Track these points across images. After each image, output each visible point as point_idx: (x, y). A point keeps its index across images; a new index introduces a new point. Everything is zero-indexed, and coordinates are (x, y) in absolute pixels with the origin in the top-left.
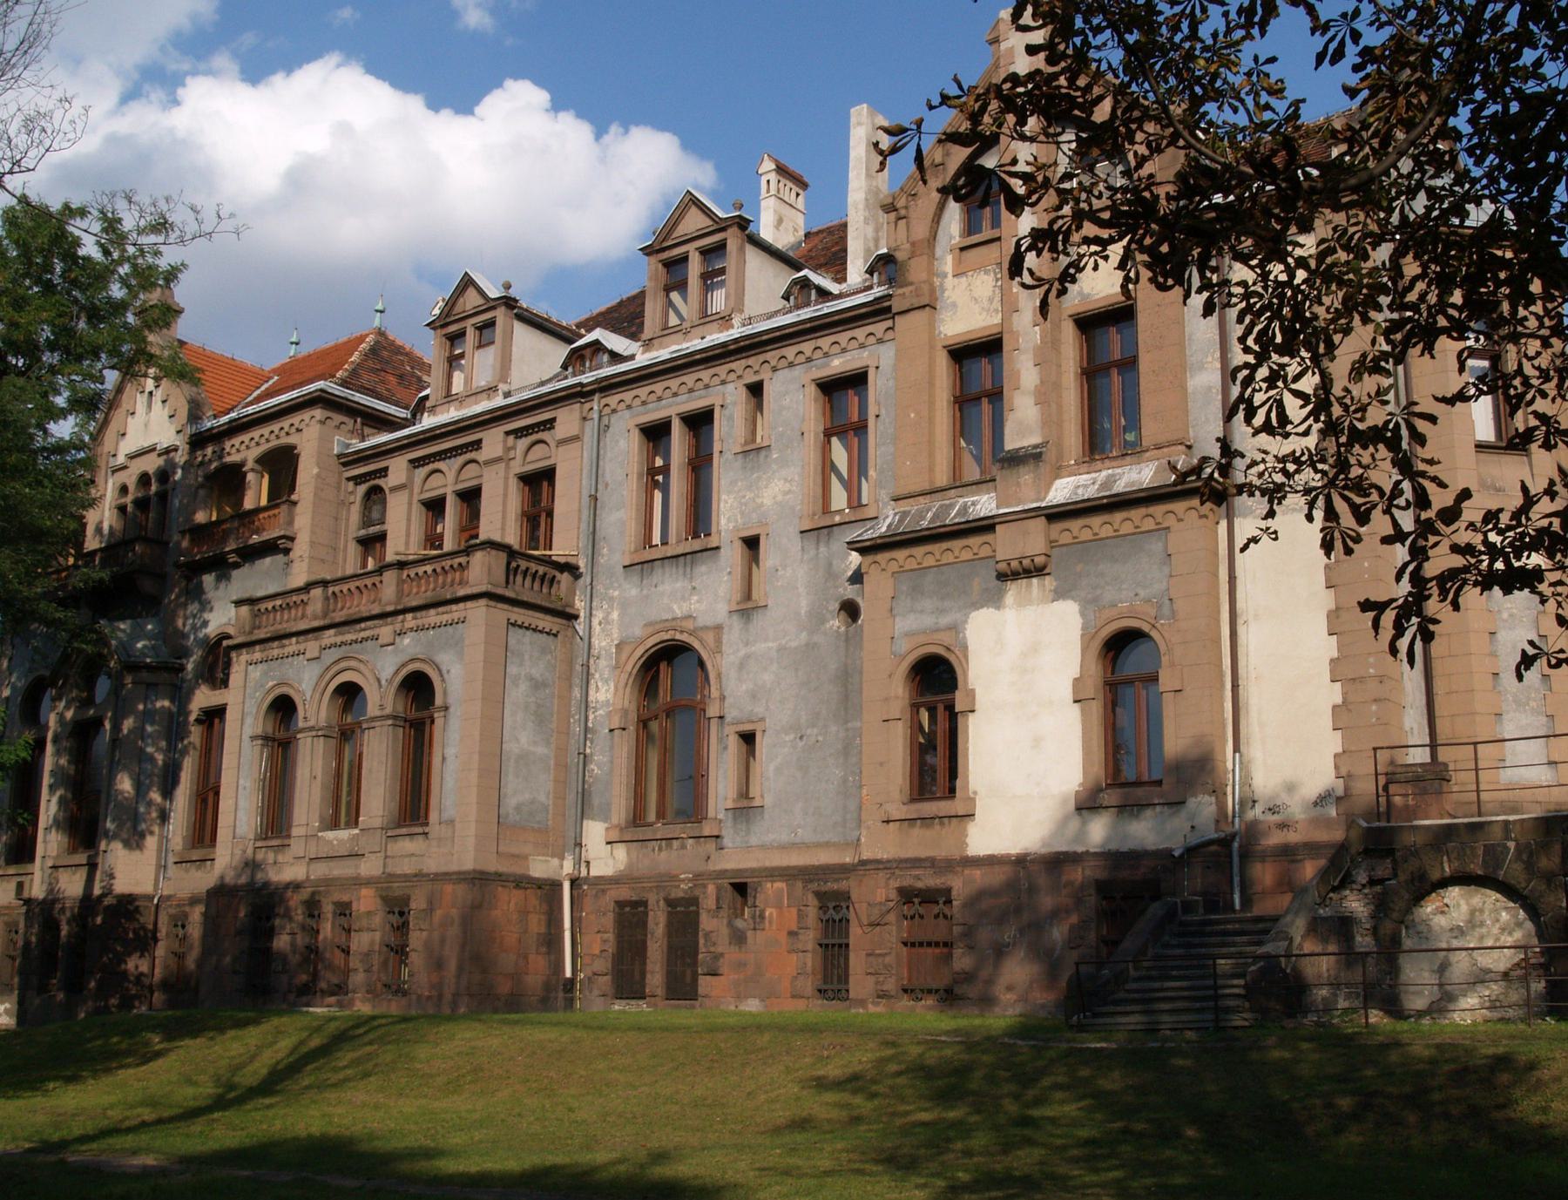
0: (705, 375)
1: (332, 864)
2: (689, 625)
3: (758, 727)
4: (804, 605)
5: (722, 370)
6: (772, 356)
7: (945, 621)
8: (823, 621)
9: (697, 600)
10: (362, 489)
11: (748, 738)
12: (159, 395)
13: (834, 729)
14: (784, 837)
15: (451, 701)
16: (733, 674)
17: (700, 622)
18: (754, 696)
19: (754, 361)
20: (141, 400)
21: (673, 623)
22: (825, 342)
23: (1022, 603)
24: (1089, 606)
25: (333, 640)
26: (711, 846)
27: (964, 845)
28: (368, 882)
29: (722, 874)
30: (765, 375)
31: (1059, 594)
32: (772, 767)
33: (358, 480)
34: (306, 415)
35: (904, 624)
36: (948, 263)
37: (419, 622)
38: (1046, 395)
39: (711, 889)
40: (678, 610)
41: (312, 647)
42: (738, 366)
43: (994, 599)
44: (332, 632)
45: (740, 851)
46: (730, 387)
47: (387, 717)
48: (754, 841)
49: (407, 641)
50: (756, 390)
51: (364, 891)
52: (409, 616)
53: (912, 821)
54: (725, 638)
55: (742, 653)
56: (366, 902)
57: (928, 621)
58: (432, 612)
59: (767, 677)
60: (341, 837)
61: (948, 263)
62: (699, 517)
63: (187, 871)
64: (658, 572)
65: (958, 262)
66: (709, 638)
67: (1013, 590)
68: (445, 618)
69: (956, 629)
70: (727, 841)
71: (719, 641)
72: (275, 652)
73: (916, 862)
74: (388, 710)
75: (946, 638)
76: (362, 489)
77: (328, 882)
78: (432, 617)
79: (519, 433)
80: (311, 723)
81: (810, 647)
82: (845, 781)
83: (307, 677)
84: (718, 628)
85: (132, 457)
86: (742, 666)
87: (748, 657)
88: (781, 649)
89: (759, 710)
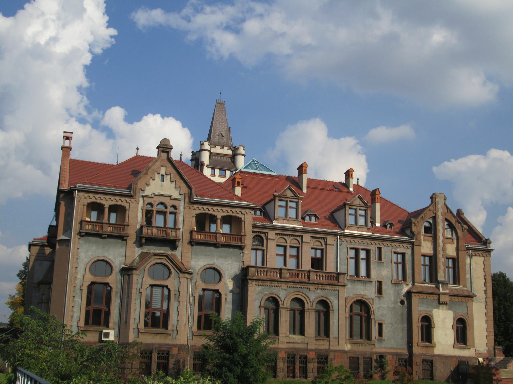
0: (368, 241)
1: (295, 345)
2: (366, 297)
3: (383, 322)
4: (393, 299)
5: (373, 242)
6: (385, 243)
7: (428, 309)
8: (397, 303)
9: (368, 292)
10: (255, 234)
11: (380, 325)
12: (167, 178)
13: (400, 325)
14: (390, 346)
15: (334, 308)
16: (377, 310)
17: (368, 297)
18: (382, 315)
19: (381, 243)
20: (158, 178)
21: (362, 296)
22: (397, 244)
23: (443, 309)
24: (455, 313)
25: (292, 286)
26: (373, 346)
27: (433, 352)
28: (312, 350)
29: (376, 353)
30: (382, 246)
31: (449, 309)
32: (386, 331)
33: (253, 232)
34: (248, 211)
35: (420, 308)
36: (422, 237)
37: (324, 288)
38: (444, 271)
39: (375, 356)
40: (362, 293)
41: (284, 286)
42: (377, 242)
43: (438, 308)
44: (292, 283)
45: (380, 348)
46: (374, 246)
47: (313, 309)
48: (382, 346)
49: (319, 291)
50: (380, 249)
51: (311, 353)
52: (320, 286)
53: (423, 347)
54: (375, 302)
55: (379, 306)
56: (311, 355)
57: (425, 309)
58: (328, 286)
59: (385, 312)
60: (297, 338)
61: (422, 237)
62: (368, 274)
63: (201, 338)
64: (356, 283)
65: (424, 239)
66: (371, 301)
67: (441, 306)
68: (332, 289)
69: (431, 311)
70: (376, 346)
71: (373, 302)
72: (268, 284)
73: (425, 355)
74: (314, 307)
75: (429, 313)
76: (255, 234)
77: (298, 350)
78: (328, 287)
79: (312, 237)
80: (285, 306)
81: (394, 308)
82: (403, 336)
83: (285, 295)
84: (373, 299)
85: (155, 195)
86: (379, 308)
87: (380, 307)
88: (388, 307)
89: (383, 319)
